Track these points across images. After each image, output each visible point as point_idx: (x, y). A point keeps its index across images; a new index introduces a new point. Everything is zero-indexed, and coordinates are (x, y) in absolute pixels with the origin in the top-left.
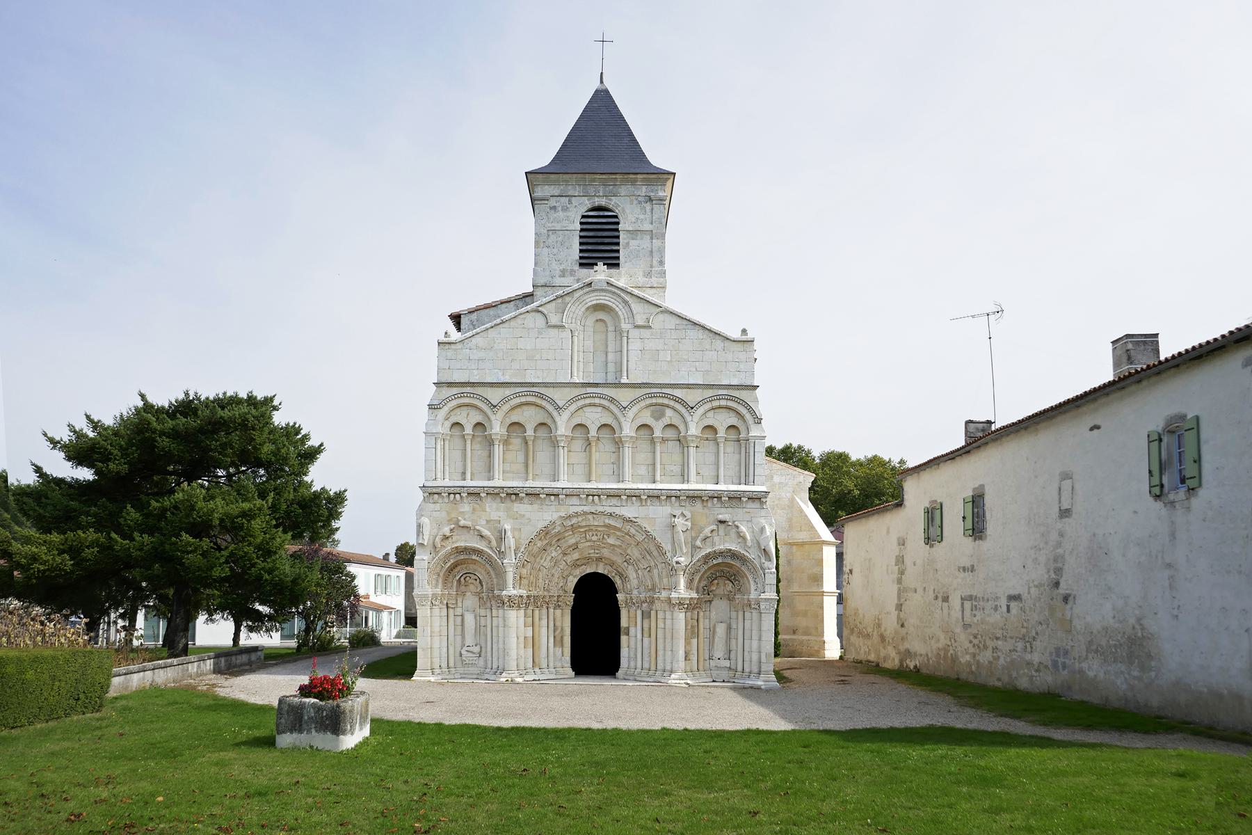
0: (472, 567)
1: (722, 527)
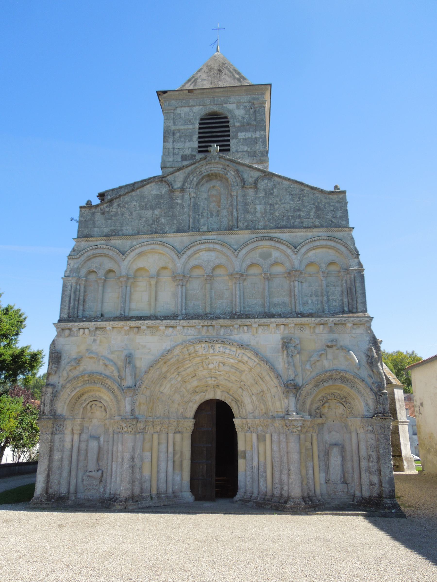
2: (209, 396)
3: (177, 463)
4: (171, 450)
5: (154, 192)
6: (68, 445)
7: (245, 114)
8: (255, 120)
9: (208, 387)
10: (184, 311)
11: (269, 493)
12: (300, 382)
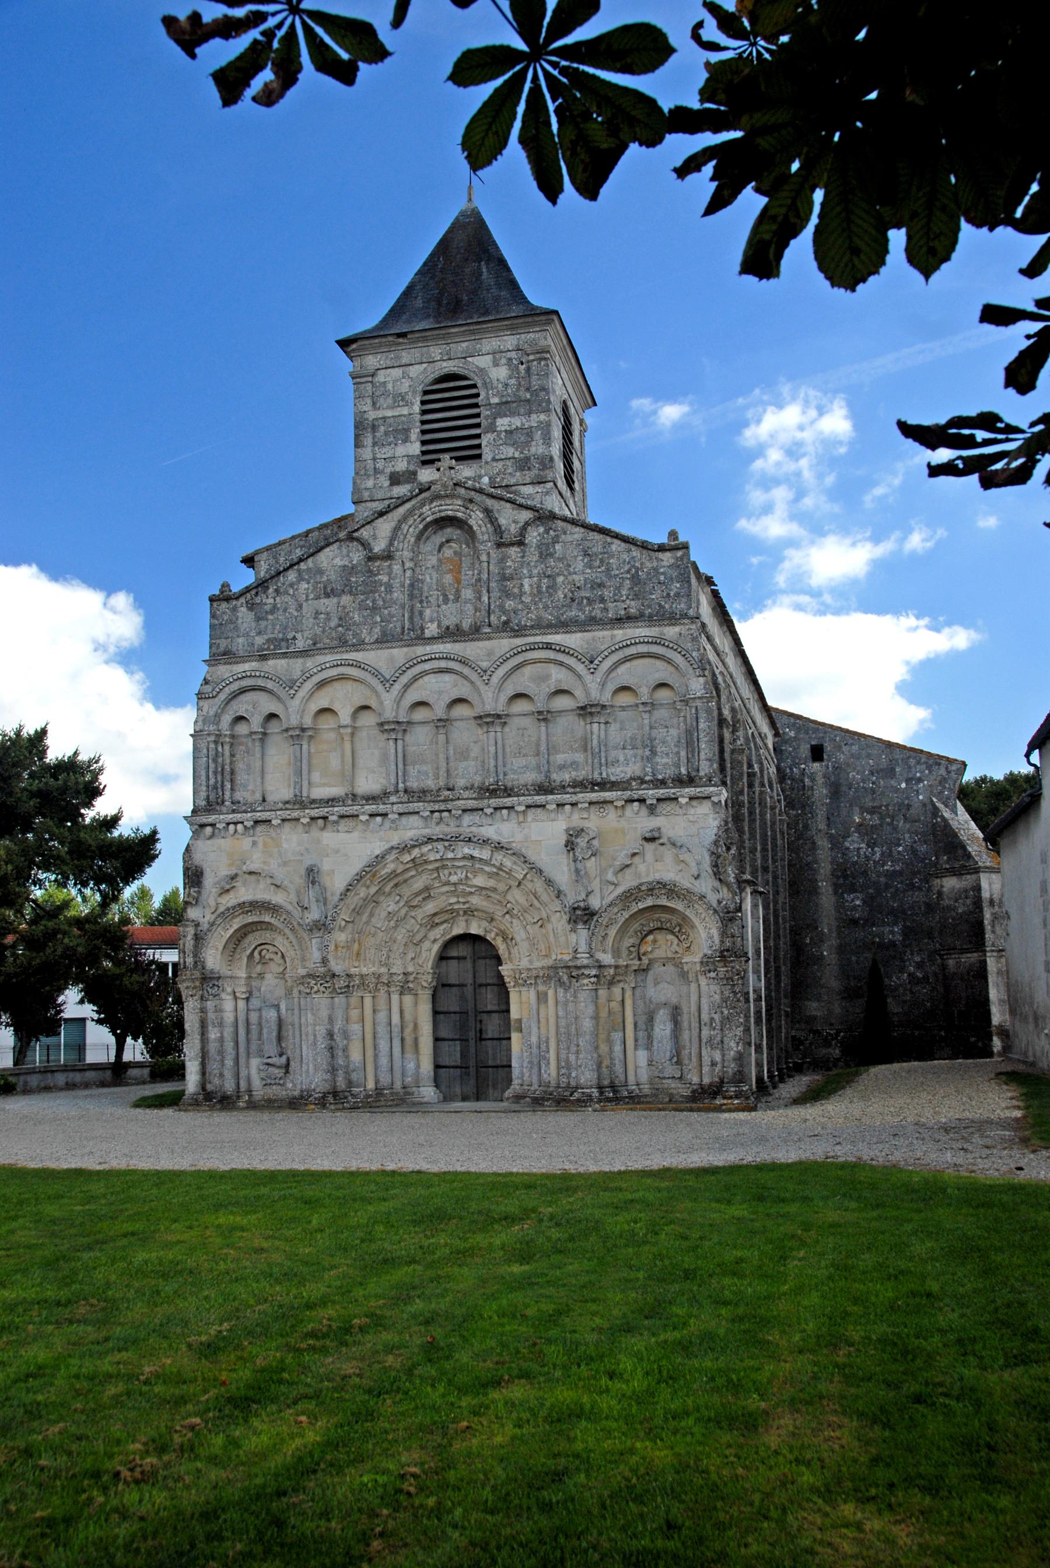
0: (267, 936)
1: (650, 847)
3: (409, 1040)
4: (396, 1019)
5: (338, 562)
6: (229, 1017)
7: (510, 378)
8: (528, 389)
10: (401, 785)
11: (553, 1083)
12: (595, 903)
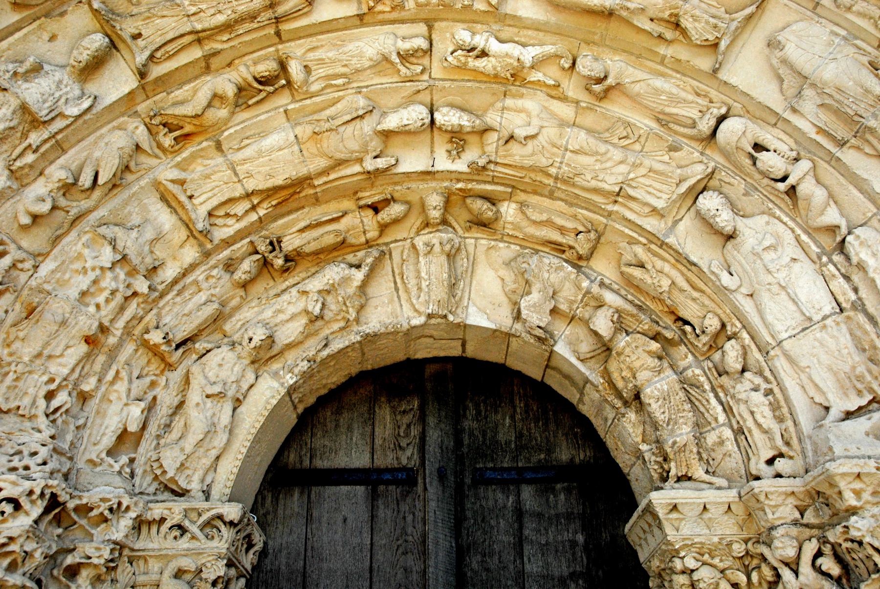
2: (405, 301)
9: (396, 210)
